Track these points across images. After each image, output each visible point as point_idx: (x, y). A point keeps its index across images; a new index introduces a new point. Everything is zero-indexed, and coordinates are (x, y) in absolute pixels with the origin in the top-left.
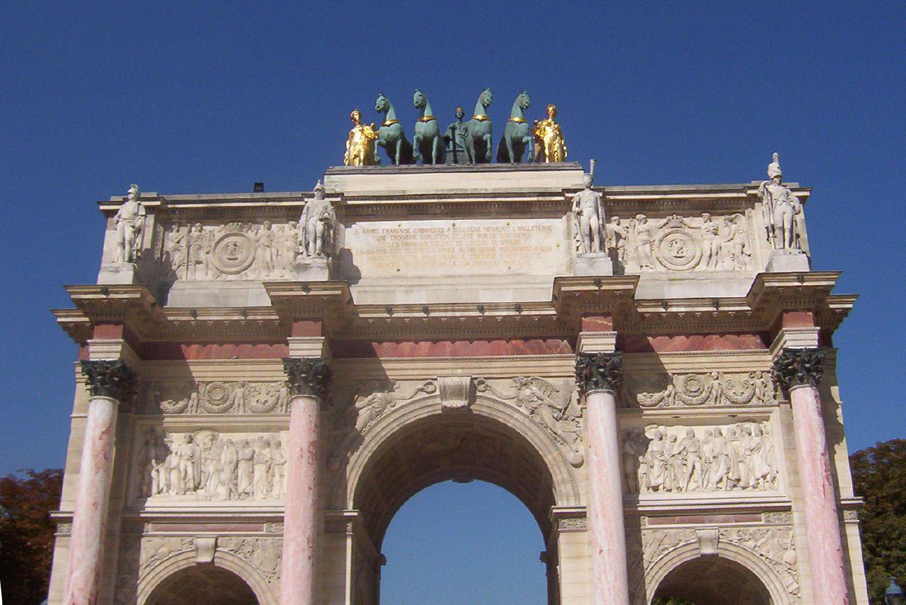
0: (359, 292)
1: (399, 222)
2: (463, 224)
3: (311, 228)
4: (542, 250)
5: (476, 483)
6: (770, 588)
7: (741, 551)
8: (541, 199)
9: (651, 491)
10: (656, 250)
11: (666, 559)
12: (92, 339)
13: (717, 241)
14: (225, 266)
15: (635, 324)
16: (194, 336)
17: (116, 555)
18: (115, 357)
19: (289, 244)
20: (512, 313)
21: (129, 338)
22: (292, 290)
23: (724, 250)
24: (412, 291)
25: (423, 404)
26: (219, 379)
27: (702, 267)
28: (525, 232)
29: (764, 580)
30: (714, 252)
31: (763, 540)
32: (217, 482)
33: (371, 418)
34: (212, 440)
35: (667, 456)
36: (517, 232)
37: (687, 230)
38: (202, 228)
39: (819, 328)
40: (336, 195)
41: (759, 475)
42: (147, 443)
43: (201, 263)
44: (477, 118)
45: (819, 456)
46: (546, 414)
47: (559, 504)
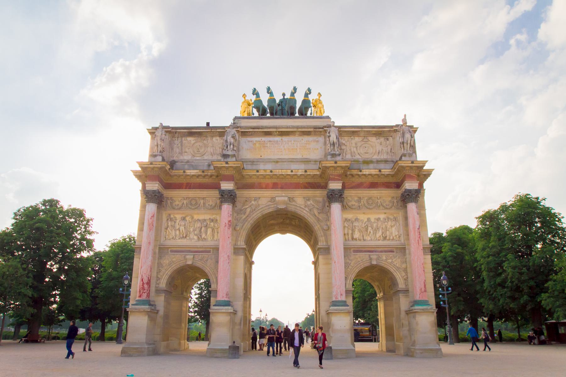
1: (261, 138)
2: (285, 139)
3: (229, 141)
6: (397, 277)
7: (386, 263)
8: (315, 130)
9: (354, 240)
10: (358, 150)
11: (359, 265)
15: (349, 178)
17: (157, 262)
18: (155, 188)
19: (220, 146)
20: (303, 173)
21: (161, 182)
25: (270, 207)
29: (395, 274)
30: (380, 151)
33: (250, 212)
34: (192, 219)
35: (360, 228)
36: (306, 142)
37: (370, 143)
38: (186, 139)
39: (418, 182)
40: (238, 127)
41: (394, 235)
42: (168, 220)
43: (187, 152)
45: (417, 229)
46: (316, 212)
47: (319, 244)
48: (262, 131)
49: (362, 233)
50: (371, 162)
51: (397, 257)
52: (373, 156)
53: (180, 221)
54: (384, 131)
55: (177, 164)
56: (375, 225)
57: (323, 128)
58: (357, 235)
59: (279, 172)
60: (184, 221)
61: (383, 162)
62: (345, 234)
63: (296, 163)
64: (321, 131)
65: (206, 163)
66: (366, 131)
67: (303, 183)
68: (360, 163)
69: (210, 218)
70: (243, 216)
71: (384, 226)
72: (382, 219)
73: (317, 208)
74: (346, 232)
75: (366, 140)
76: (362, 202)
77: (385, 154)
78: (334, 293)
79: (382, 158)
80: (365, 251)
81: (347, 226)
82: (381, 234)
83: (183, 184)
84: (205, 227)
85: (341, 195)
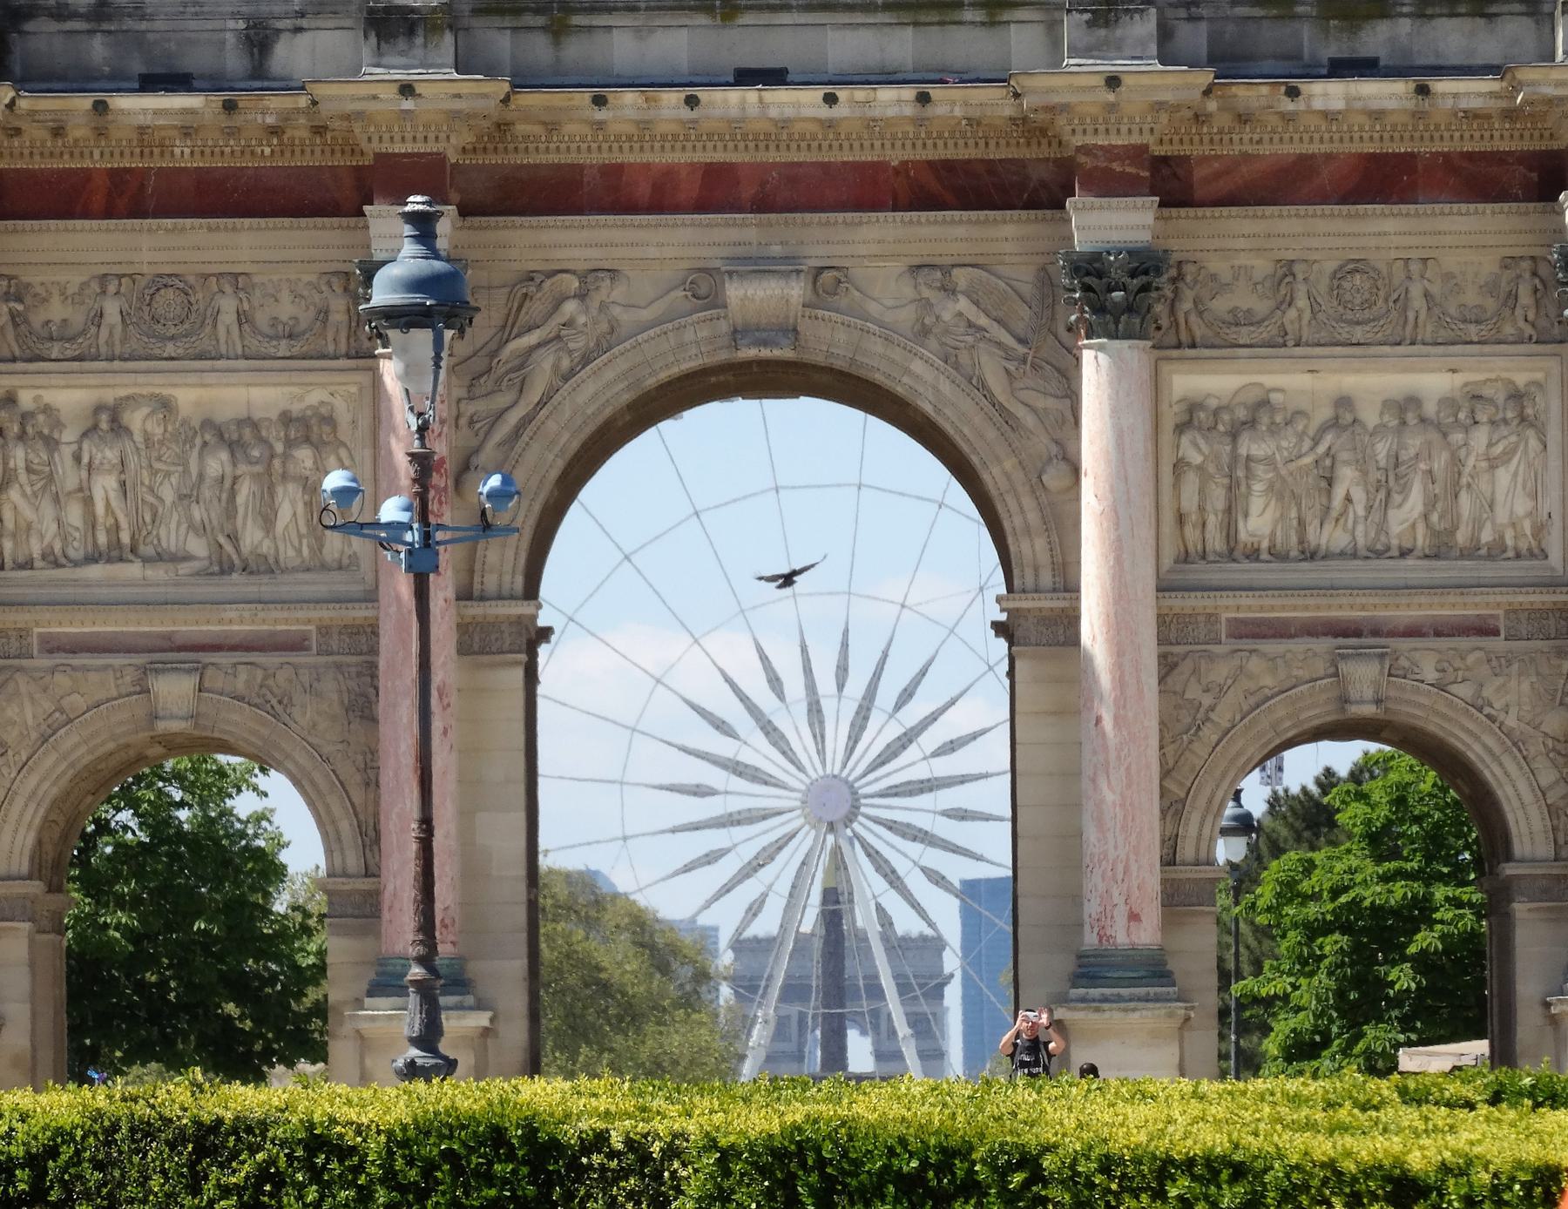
5: (804, 400)
15: (1221, 132)
16: (97, 155)
24: (652, 30)
26: (167, 270)
31: (1500, 680)
32: (185, 525)
35: (1283, 472)
49: (1299, 510)
51: (1515, 666)
53: (85, 435)
55: (29, 26)
56: (1382, 449)
58: (1259, 522)
59: (743, 101)
60: (109, 436)
62: (1181, 519)
63: (859, 18)
65: (231, 24)
67: (904, 163)
69: (286, 419)
70: (502, 400)
71: (1440, 462)
72: (1430, 409)
73: (999, 344)
74: (1190, 501)
76: (1302, 302)
78: (1092, 908)
80: (1312, 630)
81: (1196, 459)
82: (1419, 508)
83: (86, 175)
84: (256, 477)
85: (1145, 288)
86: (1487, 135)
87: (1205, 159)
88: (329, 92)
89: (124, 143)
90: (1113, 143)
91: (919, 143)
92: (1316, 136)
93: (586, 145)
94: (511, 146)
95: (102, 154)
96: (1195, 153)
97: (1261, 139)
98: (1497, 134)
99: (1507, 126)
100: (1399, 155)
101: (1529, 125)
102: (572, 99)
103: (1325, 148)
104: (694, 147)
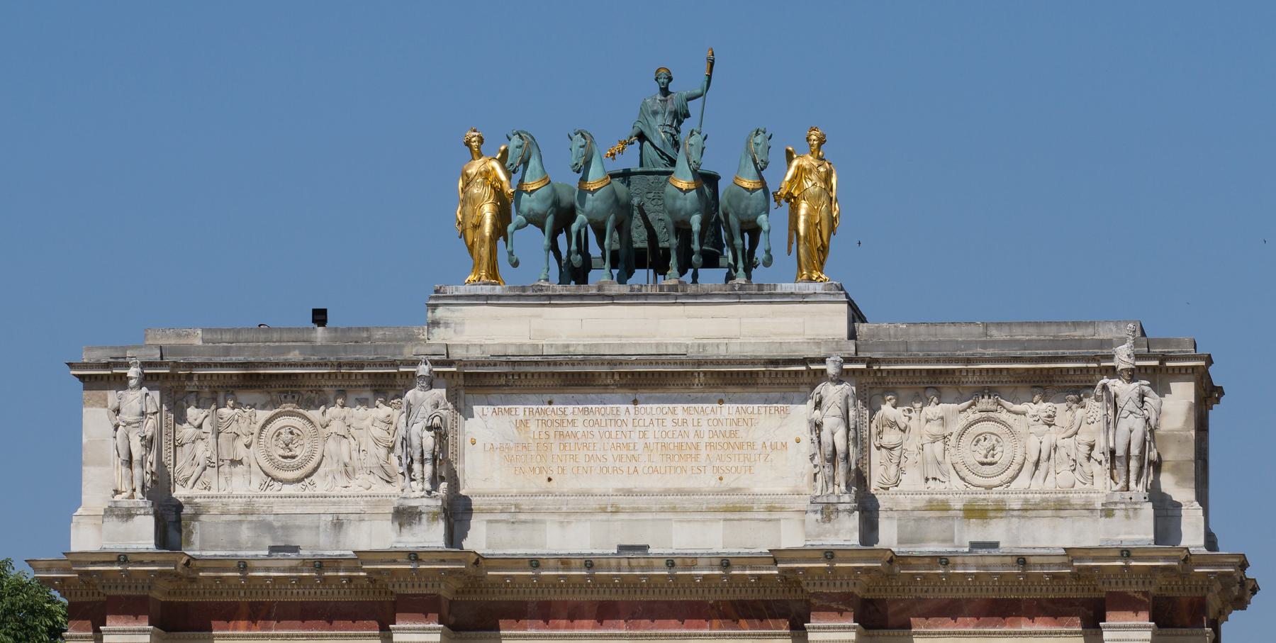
0: (489, 522)
3: (415, 442)
4: (774, 447)
12: (105, 625)
13: (1052, 436)
14: (278, 467)
16: (242, 594)
19: (378, 432)
22: (395, 562)
23: (1062, 452)
27: (1023, 481)
28: (747, 417)
30: (1044, 456)
37: (1004, 416)
43: (240, 462)
44: (679, 185)
48: (553, 374)
50: (1001, 509)
52: (1014, 478)
54: (1061, 369)
55: (203, 518)
57: (804, 361)
61: (1049, 513)
64: (796, 372)
65: (323, 517)
66: (987, 370)
68: (953, 518)
75: (994, 407)
77: (1065, 469)
79: (1050, 485)
86: (1062, 588)
87: (895, 601)
88: (367, 558)
89: (258, 587)
90: (832, 591)
91: (725, 590)
92: (961, 588)
93: (658, 589)
94: (485, 590)
95: (245, 593)
96: (889, 597)
97: (928, 589)
98: (1068, 588)
99: (1074, 583)
100: (1008, 600)
101: (1087, 583)
102: (519, 563)
103: (966, 595)
104: (946, 589)
